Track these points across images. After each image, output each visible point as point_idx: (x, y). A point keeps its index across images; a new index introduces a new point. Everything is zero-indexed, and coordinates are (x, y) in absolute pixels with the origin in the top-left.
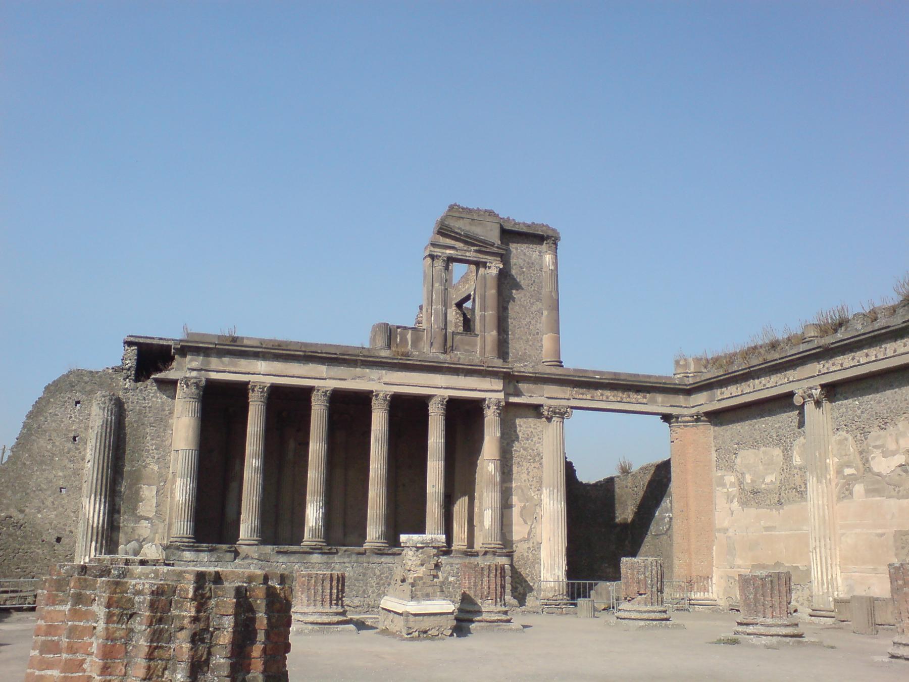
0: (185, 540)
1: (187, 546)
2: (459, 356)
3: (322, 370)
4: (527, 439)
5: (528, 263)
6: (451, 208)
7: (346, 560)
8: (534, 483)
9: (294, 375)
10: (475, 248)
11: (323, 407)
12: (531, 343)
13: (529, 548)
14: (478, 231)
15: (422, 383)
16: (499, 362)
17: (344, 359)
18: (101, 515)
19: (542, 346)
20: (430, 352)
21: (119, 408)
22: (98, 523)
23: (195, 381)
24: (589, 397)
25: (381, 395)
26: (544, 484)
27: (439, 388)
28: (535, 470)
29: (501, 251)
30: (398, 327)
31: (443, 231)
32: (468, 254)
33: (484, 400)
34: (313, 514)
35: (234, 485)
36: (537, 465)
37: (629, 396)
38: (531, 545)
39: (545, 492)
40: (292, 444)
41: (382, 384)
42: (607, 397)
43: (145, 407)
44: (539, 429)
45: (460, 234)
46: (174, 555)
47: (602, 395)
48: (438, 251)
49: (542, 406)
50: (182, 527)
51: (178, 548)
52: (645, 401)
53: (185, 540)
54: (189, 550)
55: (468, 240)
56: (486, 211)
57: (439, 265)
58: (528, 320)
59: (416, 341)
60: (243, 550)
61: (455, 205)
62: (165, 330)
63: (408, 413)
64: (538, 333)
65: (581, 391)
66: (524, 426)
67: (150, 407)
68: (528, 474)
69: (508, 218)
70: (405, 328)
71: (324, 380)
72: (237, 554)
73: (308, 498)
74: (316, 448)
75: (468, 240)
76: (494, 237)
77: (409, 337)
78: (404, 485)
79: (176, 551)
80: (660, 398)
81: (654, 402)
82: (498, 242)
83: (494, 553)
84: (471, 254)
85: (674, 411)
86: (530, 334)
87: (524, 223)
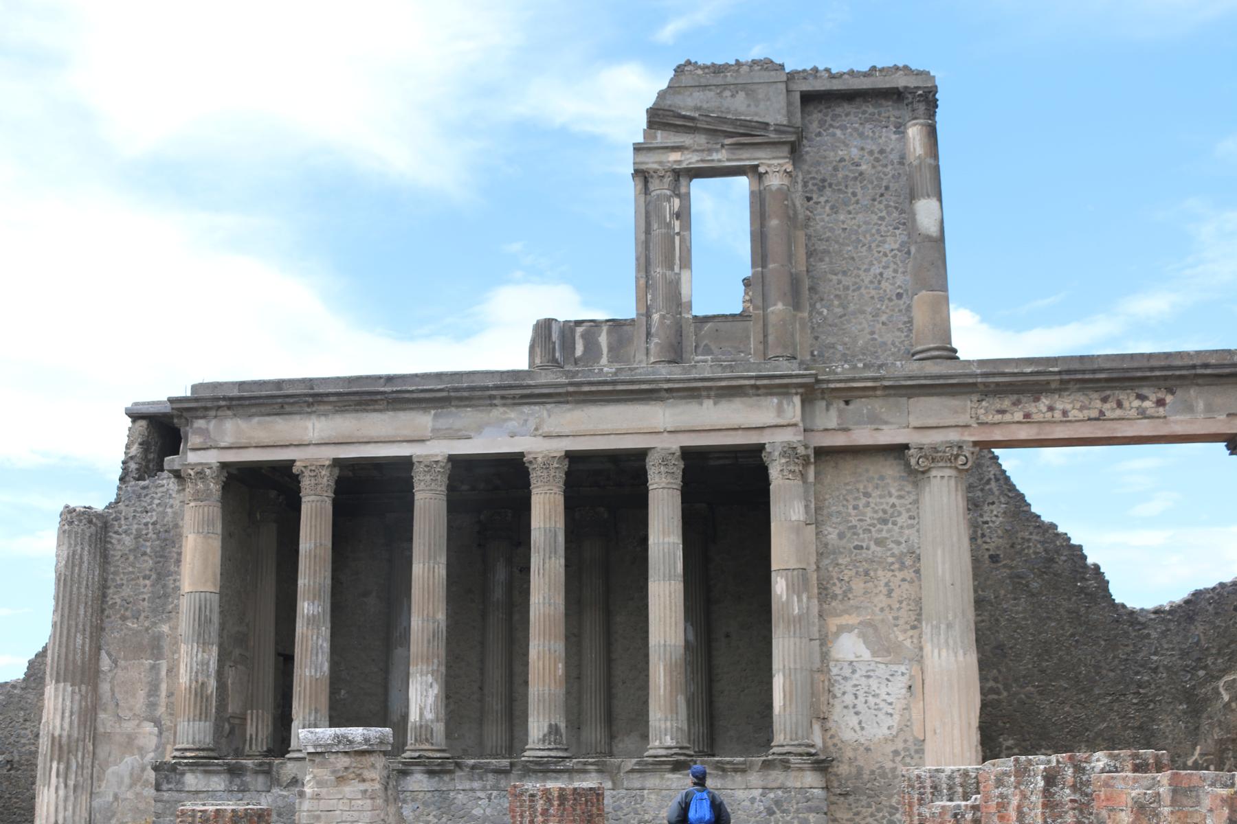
0: (188, 754)
1: (186, 764)
2: (703, 366)
3: (423, 421)
4: (885, 522)
5: (871, 153)
6: (679, 70)
7: (476, 785)
8: (903, 613)
9: (378, 437)
10: (728, 141)
11: (428, 495)
12: (884, 318)
13: (896, 753)
14: (739, 106)
15: (624, 426)
17: (461, 399)
18: (67, 714)
19: (911, 322)
20: (646, 363)
22: (62, 728)
23: (200, 468)
24: (1019, 416)
25: (540, 460)
26: (924, 617)
28: (906, 585)
29: (785, 138)
30: (579, 323)
32: (715, 156)
33: (761, 447)
34: (422, 697)
35: (399, 651)
36: (909, 574)
37: (1120, 405)
38: (900, 745)
39: (926, 628)
40: (500, 574)
41: (541, 438)
42: (1065, 413)
43: (146, 524)
44: (913, 497)
45: (692, 119)
46: (168, 782)
47: (1051, 409)
48: (651, 162)
49: (906, 447)
50: (192, 732)
51: (173, 768)
52: (1161, 409)
53: (188, 754)
54: (193, 772)
56: (754, 62)
57: (660, 188)
58: (876, 269)
59: (617, 351)
61: (689, 63)
63: (606, 490)
64: (899, 296)
65: (998, 404)
66: (876, 493)
67: (154, 524)
68: (889, 595)
69: (815, 70)
70: (595, 323)
71: (428, 442)
73: (412, 669)
74: (428, 570)
76: (774, 110)
77: (603, 339)
78: (727, 636)
79: (173, 775)
80: (1199, 398)
81: (1190, 409)
83: (786, 766)
84: (721, 157)
86: (881, 299)
87: (852, 73)
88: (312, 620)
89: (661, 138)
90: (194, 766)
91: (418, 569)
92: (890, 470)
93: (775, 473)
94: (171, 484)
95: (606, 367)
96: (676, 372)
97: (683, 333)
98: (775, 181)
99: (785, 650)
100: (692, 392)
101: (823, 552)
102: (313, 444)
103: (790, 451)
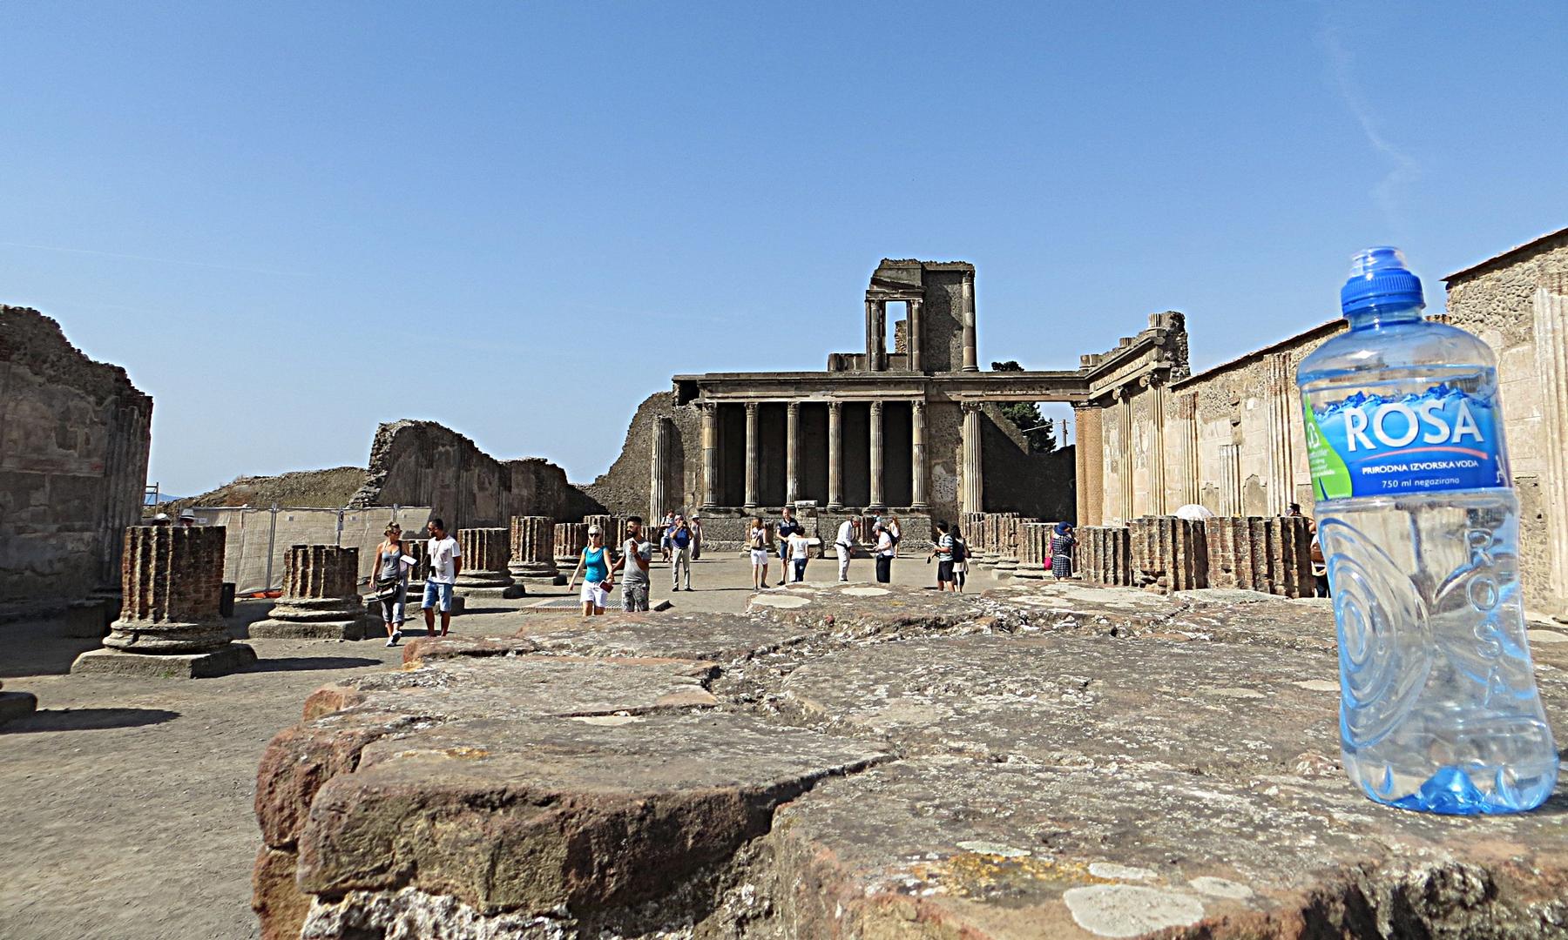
2: (891, 373)
9: (776, 396)
16: (921, 375)
20: (873, 373)
21: (668, 424)
27: (876, 395)
31: (874, 281)
55: (895, 286)
57: (874, 307)
59: (859, 366)
60: (747, 511)
62: (697, 370)
63: (854, 415)
72: (743, 514)
75: (895, 286)
82: (919, 283)
85: (1075, 399)
88: (754, 459)
89: (876, 288)
90: (712, 511)
91: (790, 442)
92: (954, 409)
93: (915, 410)
94: (694, 408)
95: (855, 372)
96: (881, 375)
97: (883, 362)
98: (916, 306)
99: (916, 471)
100: (887, 383)
101: (930, 436)
102: (752, 397)
103: (920, 404)
